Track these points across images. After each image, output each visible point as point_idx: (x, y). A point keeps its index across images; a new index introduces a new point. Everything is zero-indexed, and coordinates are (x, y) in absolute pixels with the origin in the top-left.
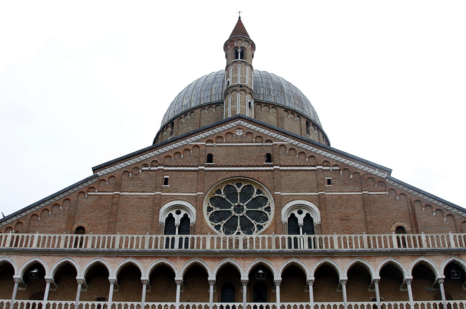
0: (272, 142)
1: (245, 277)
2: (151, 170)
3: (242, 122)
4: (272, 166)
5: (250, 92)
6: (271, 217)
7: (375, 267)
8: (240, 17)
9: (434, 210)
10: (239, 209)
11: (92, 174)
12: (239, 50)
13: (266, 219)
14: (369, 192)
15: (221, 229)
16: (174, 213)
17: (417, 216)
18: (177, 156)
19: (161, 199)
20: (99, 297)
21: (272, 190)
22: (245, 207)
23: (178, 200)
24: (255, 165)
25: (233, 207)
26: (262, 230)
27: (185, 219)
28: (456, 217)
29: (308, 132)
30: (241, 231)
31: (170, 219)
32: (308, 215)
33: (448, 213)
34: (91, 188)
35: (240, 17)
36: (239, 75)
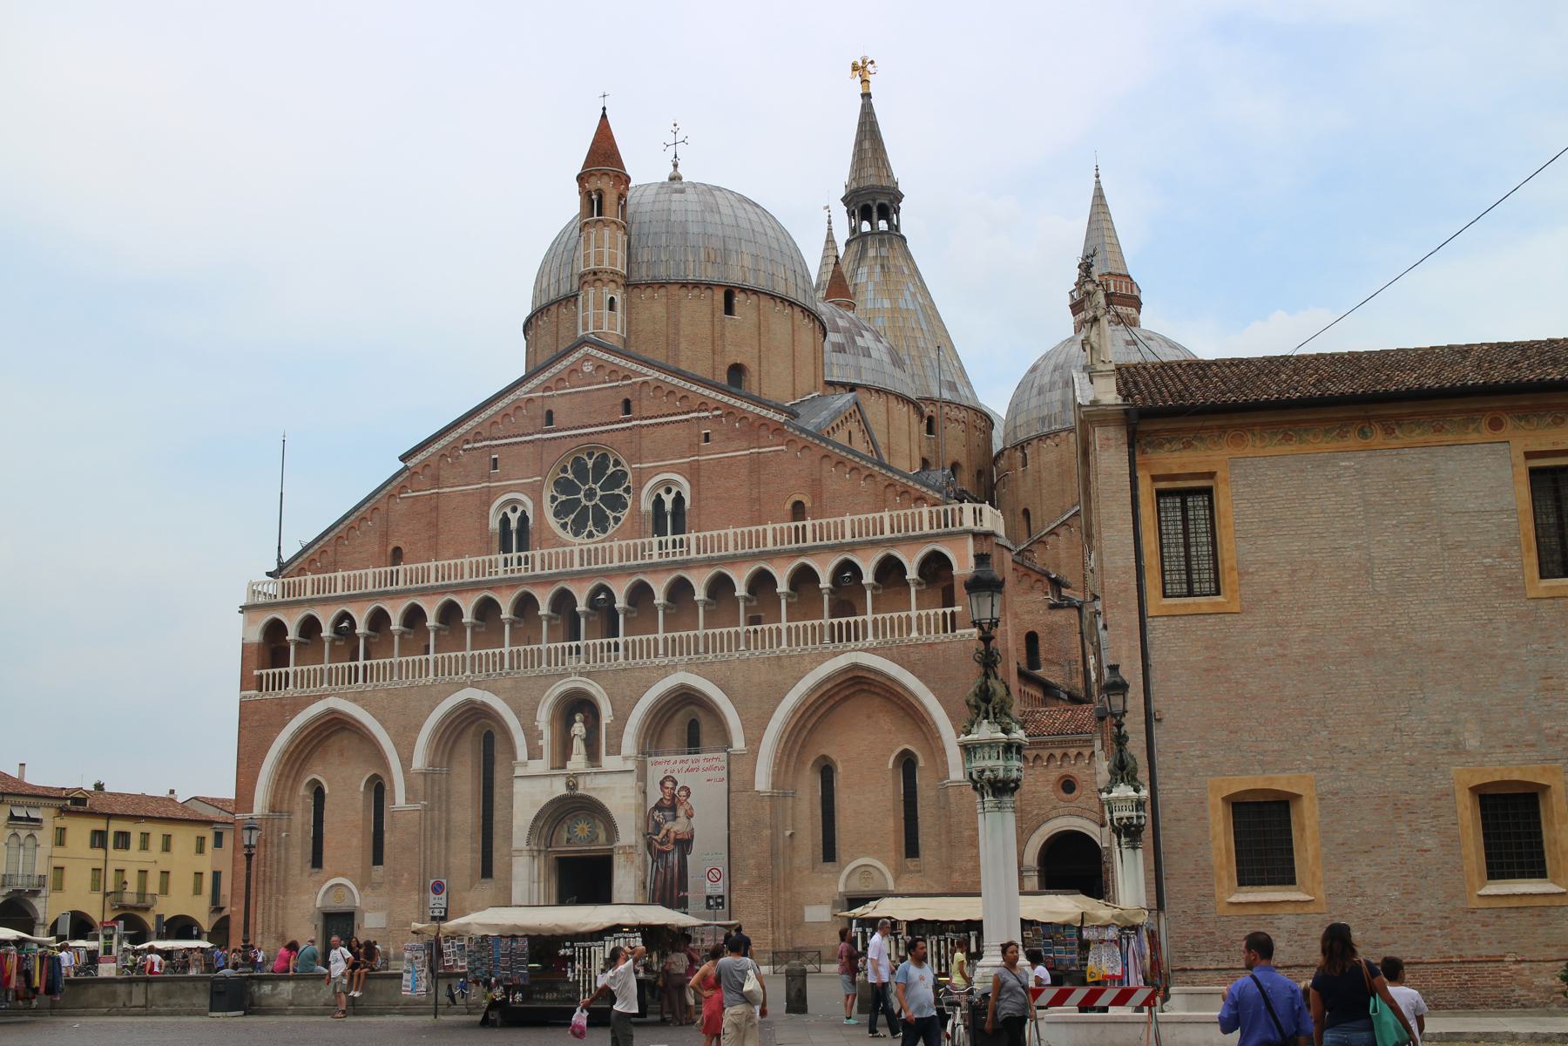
1: (581, 607)
2: (475, 449)
7: (740, 578)
8: (604, 109)
9: (848, 470)
10: (590, 494)
11: (402, 465)
12: (594, 197)
13: (625, 506)
14: (759, 448)
15: (569, 527)
16: (508, 510)
18: (506, 420)
19: (489, 491)
21: (630, 462)
22: (598, 490)
23: (511, 491)
25: (582, 493)
26: (620, 523)
27: (523, 519)
28: (878, 479)
29: (729, 309)
30: (592, 529)
31: (505, 521)
32: (679, 493)
33: (867, 473)
34: (403, 488)
35: (604, 109)
36: (592, 250)
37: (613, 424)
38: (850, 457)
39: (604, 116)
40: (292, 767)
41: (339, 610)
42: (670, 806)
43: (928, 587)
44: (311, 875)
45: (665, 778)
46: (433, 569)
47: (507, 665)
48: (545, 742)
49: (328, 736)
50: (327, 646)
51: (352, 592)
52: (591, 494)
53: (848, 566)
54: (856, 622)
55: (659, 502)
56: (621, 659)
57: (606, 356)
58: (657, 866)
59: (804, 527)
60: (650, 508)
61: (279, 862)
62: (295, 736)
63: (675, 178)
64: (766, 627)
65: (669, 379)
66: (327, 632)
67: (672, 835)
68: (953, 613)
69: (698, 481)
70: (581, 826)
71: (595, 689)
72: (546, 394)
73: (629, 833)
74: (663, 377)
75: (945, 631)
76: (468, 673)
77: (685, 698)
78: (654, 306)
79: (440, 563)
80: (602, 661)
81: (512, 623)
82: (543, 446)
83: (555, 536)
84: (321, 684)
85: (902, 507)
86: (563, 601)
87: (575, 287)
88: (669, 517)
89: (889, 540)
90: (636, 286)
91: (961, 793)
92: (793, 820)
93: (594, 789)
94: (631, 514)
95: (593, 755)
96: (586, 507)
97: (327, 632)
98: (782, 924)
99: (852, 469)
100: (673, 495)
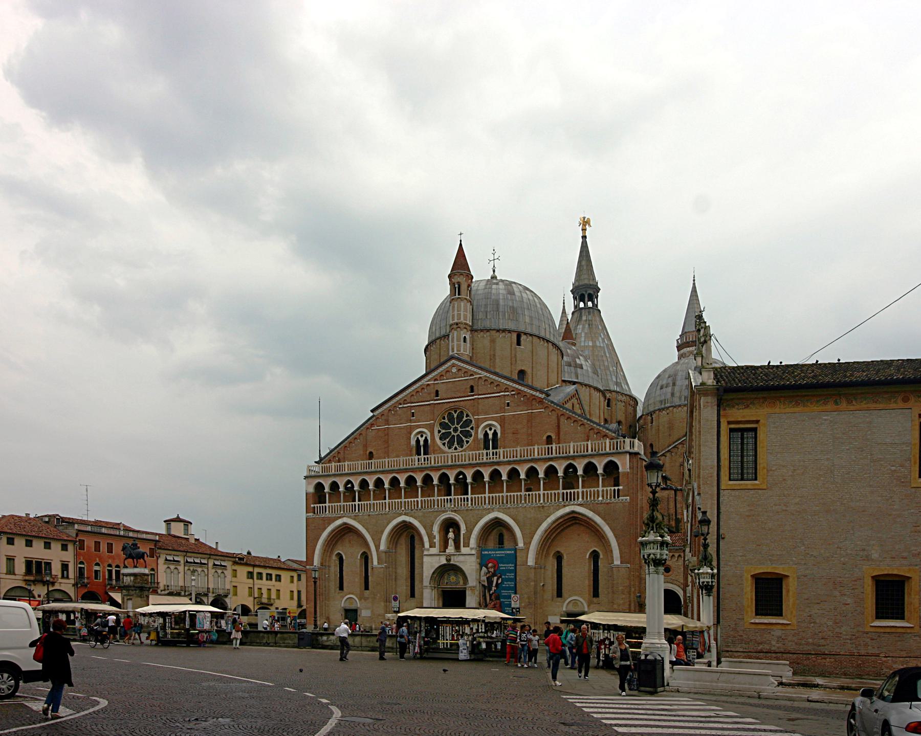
1: (452, 481)
2: (405, 407)
4: (473, 396)
5: (464, 326)
7: (522, 470)
10: (456, 430)
11: (372, 414)
13: (471, 436)
17: (561, 427)
18: (418, 394)
24: (463, 395)
27: (426, 440)
28: (587, 426)
31: (418, 441)
32: (495, 431)
34: (372, 425)
38: (574, 415)
40: (330, 546)
41: (346, 480)
43: (607, 477)
44: (339, 593)
46: (387, 462)
47: (420, 506)
48: (437, 540)
49: (344, 535)
50: (342, 495)
51: (352, 471)
52: (456, 430)
53: (571, 466)
54: (574, 492)
55: (486, 435)
56: (470, 505)
57: (462, 365)
59: (552, 448)
60: (482, 437)
61: (325, 587)
63: (494, 277)
64: (534, 493)
65: (491, 376)
66: (342, 489)
68: (618, 490)
69: (504, 425)
71: (458, 518)
72: (436, 382)
74: (488, 375)
75: (614, 497)
76: (403, 509)
77: (497, 523)
78: (484, 340)
79: (390, 460)
80: (461, 505)
81: (422, 487)
82: (434, 407)
84: (340, 511)
85: (597, 439)
86: (444, 478)
87: (448, 331)
89: (590, 455)
90: (476, 331)
91: (619, 570)
92: (544, 578)
93: (458, 562)
94: (474, 440)
95: (457, 547)
96: (454, 436)
97: (342, 489)
98: (538, 623)
99: (575, 421)
100: (493, 431)
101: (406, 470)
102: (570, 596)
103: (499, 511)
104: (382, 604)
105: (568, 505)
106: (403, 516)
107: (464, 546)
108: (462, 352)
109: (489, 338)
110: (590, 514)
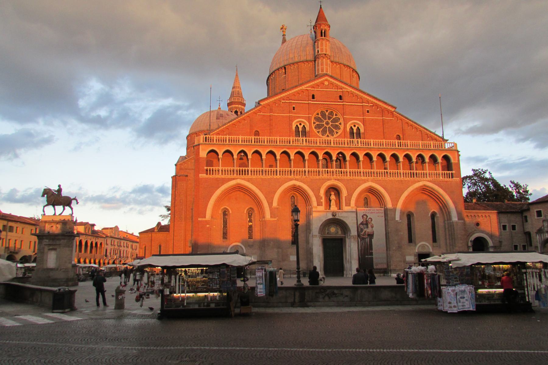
0: (342, 89)
2: (286, 102)
3: (328, 78)
4: (343, 102)
6: (342, 127)
7: (388, 155)
8: (321, 6)
10: (327, 123)
12: (323, 31)
20: (270, 164)
21: (343, 114)
22: (330, 122)
23: (300, 118)
24: (334, 101)
28: (423, 132)
31: (297, 127)
35: (321, 6)
36: (324, 47)
37: (336, 102)
39: (321, 8)
42: (366, 223)
45: (364, 215)
48: (323, 200)
52: (327, 123)
58: (362, 243)
62: (223, 192)
67: (367, 233)
68: (452, 174)
70: (332, 229)
71: (340, 185)
73: (354, 232)
74: (353, 90)
77: (371, 190)
83: (317, 135)
88: (355, 134)
91: (457, 225)
93: (342, 217)
101: (296, 147)
102: (420, 242)
103: (372, 182)
104: (276, 250)
105: (421, 181)
106: (294, 181)
107: (346, 206)
108: (329, 73)
109: (339, 68)
110: (436, 187)
